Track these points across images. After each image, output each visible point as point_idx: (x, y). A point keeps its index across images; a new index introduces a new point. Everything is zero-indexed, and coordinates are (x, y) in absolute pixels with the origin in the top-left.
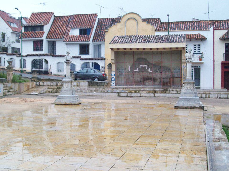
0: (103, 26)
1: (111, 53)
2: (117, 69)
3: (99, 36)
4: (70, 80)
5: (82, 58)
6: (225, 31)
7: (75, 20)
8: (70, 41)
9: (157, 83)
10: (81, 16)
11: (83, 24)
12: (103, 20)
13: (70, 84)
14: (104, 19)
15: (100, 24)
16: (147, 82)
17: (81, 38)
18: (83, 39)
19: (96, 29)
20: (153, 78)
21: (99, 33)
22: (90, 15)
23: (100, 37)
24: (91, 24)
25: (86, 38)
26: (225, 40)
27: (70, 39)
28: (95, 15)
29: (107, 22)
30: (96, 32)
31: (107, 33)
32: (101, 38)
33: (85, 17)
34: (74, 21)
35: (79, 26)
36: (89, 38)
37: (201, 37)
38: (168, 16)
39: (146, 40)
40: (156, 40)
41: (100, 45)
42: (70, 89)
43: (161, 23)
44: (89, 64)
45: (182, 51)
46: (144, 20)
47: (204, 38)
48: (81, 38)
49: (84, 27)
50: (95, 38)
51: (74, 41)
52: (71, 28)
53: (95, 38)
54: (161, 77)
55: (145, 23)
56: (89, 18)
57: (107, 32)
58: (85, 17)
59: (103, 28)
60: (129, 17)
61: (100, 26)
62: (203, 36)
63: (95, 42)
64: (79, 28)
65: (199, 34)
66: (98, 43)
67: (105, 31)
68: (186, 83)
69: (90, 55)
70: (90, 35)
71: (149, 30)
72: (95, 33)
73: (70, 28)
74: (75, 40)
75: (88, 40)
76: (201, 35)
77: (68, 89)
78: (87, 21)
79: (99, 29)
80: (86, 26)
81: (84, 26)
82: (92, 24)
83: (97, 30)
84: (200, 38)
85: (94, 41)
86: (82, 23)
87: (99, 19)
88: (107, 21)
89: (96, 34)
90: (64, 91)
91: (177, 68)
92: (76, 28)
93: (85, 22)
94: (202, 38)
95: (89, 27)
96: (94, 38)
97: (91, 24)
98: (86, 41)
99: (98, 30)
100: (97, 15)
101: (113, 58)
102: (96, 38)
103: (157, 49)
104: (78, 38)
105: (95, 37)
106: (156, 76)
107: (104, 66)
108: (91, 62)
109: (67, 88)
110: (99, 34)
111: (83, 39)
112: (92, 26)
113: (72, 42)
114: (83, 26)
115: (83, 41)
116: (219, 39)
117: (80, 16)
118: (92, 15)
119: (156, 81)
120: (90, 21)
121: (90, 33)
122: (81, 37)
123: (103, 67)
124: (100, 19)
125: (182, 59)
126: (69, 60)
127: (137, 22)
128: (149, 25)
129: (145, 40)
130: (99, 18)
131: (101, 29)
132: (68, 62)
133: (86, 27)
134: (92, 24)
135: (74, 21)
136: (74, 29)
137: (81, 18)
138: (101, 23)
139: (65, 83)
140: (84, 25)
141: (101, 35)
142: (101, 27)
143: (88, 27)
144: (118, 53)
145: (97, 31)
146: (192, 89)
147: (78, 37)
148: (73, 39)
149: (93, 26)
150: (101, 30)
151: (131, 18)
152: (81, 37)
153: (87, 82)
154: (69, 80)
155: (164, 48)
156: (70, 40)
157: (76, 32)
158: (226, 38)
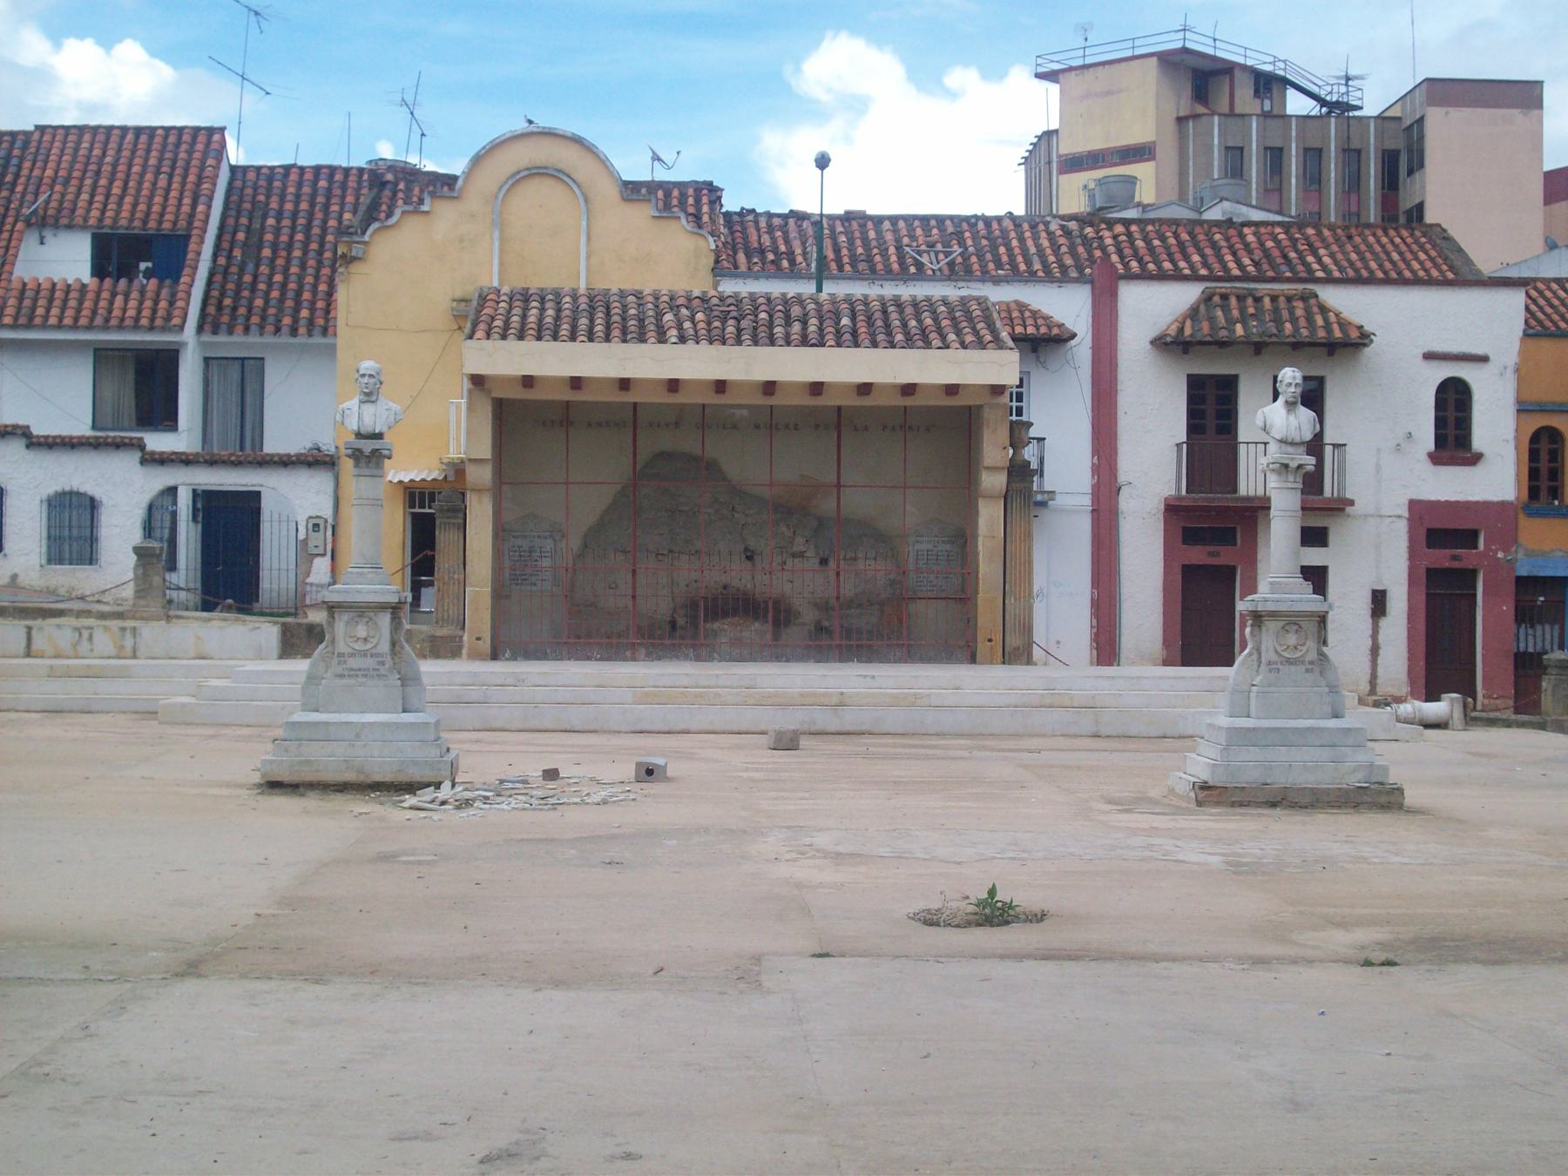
0: (271, 221)
1: (471, 408)
3: (246, 293)
4: (389, 592)
5: (153, 453)
6: (1190, 294)
7: (51, 165)
8: (30, 326)
9: (794, 634)
10: (101, 137)
11: (122, 198)
12: (267, 176)
13: (385, 619)
14: (272, 168)
15: (247, 206)
16: (726, 629)
17: (119, 299)
18: (131, 313)
19: (219, 237)
20: (777, 603)
21: (242, 271)
22: (172, 139)
23: (259, 302)
24: (187, 201)
25: (156, 302)
26: (1186, 352)
27: (27, 303)
28: (209, 143)
29: (298, 196)
30: (222, 261)
31: (356, 268)
32: (264, 310)
33: (133, 152)
34: (49, 172)
35: (89, 211)
36: (180, 304)
37: (1037, 328)
38: (823, 162)
39: (724, 321)
40: (797, 327)
42: (388, 661)
43: (727, 215)
44: (175, 503)
45: (987, 413)
46: (633, 191)
47: (1055, 331)
48: (111, 303)
49: (125, 219)
50: (220, 307)
51: (59, 327)
52: (29, 224)
53: (220, 307)
55: (641, 214)
56: (161, 160)
57: (354, 259)
58: (133, 152)
59: (269, 237)
60: (524, 163)
61: (244, 221)
62: (1046, 318)
63: (222, 338)
64: (84, 227)
65: (1022, 307)
66: (234, 344)
67: (344, 256)
68: (1274, 615)
69: (184, 435)
70: (183, 280)
71: (675, 261)
72: (211, 275)
73: (20, 226)
74: (69, 313)
75: (168, 318)
76: (1035, 314)
77: (369, 663)
78: (149, 176)
79: (245, 244)
80: (148, 214)
81: (133, 213)
82: (194, 205)
83: (226, 245)
84: (1030, 330)
85: (207, 327)
86: (116, 191)
87: (233, 169)
88: (300, 185)
89: (218, 278)
90: (341, 676)
92: (70, 227)
93: (131, 184)
94: (1043, 330)
95: (167, 225)
96: (211, 310)
97: (187, 201)
98: (158, 322)
99: (237, 253)
101: (485, 450)
102: (227, 311)
103: (817, 388)
104: (88, 304)
105: (213, 301)
106: (787, 588)
107: (327, 512)
108: (189, 480)
109: (364, 654)
110: (248, 278)
111: (131, 313)
112: (192, 215)
113: (44, 326)
114: (125, 214)
115: (136, 327)
116: (1149, 346)
117: (87, 137)
118: (186, 138)
119: (788, 623)
120: (177, 179)
121: (187, 271)
122: (114, 295)
123: (321, 523)
124: (245, 169)
126: (379, 436)
127: (581, 200)
128: (673, 225)
129: (717, 324)
130: (233, 162)
131: (253, 246)
132: (374, 451)
133: (145, 222)
134: (194, 205)
135: (49, 172)
136: (48, 233)
137: (96, 152)
138: (254, 203)
139: (345, 617)
140: (127, 207)
141: (262, 286)
142: (256, 225)
143: (160, 222)
144: (517, 415)
145: (229, 257)
146: (1311, 663)
147: (90, 296)
148: (55, 311)
149: (200, 216)
150: (260, 248)
151: (538, 172)
152: (114, 295)
153: (276, 623)
154: (383, 593)
155: (865, 389)
156: (31, 318)
157: (65, 259)
158: (1199, 337)
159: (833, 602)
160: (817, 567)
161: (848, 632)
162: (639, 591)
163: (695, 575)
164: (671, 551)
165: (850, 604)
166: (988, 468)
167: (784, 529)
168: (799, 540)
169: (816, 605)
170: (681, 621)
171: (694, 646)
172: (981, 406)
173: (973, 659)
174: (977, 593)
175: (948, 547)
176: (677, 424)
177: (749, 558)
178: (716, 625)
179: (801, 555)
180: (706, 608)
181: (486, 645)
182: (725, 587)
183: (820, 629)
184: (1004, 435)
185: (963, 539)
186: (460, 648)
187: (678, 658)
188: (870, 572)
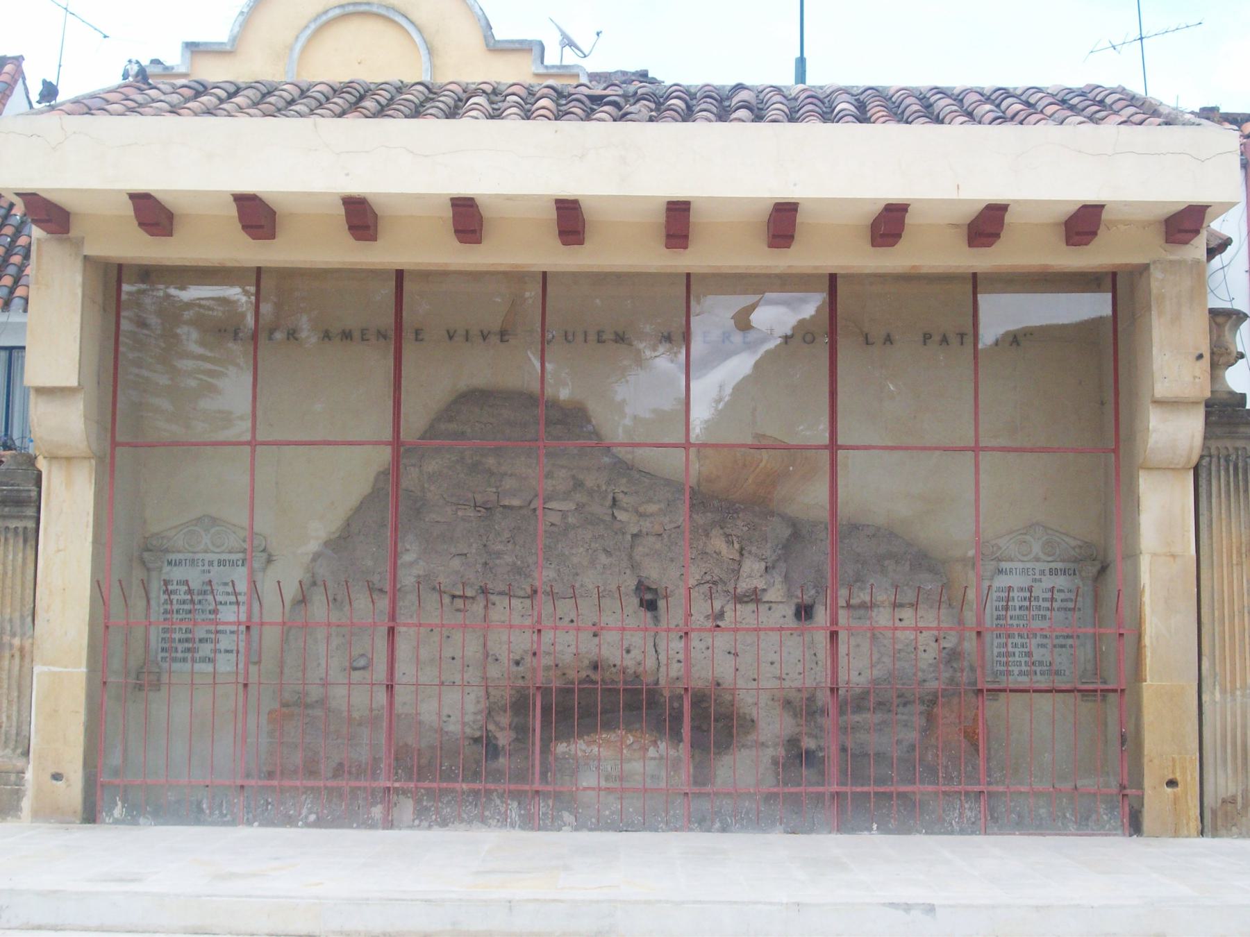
2: (133, 557)
9: (744, 768)
16: (597, 757)
20: (700, 700)
41: (15, 353)
54: (819, 677)
91: (1037, 549)
100: (19, 74)
106: (724, 669)
125: (1162, 389)
127: (423, 51)
159: (823, 698)
160: (791, 622)
161: (857, 762)
162: (405, 669)
163: (523, 642)
164: (484, 591)
165: (860, 702)
166: (1159, 403)
167: (717, 543)
168: (752, 567)
169: (787, 703)
170: (504, 739)
171: (517, 795)
172: (1146, 267)
173: (1135, 826)
174: (1138, 674)
175: (1061, 581)
176: (503, 335)
177: (651, 606)
178: (580, 747)
179: (754, 597)
180: (546, 710)
181: (73, 791)
182: (595, 667)
183: (798, 757)
184: (1197, 335)
185: (1099, 567)
186: (18, 794)
187: (483, 820)
188: (895, 639)
